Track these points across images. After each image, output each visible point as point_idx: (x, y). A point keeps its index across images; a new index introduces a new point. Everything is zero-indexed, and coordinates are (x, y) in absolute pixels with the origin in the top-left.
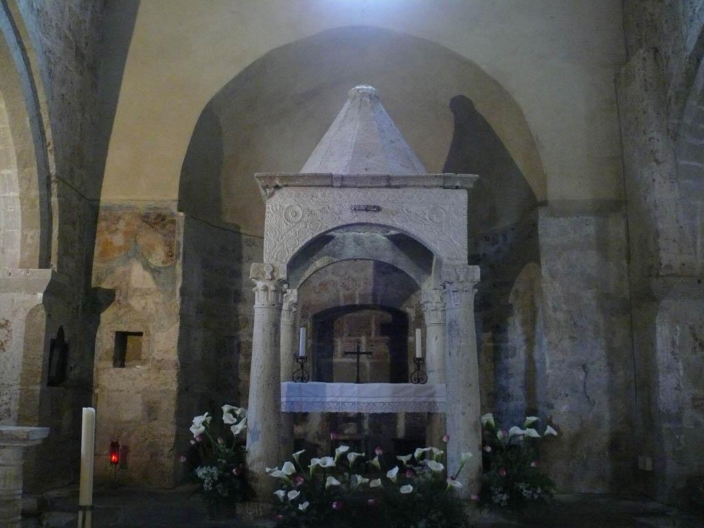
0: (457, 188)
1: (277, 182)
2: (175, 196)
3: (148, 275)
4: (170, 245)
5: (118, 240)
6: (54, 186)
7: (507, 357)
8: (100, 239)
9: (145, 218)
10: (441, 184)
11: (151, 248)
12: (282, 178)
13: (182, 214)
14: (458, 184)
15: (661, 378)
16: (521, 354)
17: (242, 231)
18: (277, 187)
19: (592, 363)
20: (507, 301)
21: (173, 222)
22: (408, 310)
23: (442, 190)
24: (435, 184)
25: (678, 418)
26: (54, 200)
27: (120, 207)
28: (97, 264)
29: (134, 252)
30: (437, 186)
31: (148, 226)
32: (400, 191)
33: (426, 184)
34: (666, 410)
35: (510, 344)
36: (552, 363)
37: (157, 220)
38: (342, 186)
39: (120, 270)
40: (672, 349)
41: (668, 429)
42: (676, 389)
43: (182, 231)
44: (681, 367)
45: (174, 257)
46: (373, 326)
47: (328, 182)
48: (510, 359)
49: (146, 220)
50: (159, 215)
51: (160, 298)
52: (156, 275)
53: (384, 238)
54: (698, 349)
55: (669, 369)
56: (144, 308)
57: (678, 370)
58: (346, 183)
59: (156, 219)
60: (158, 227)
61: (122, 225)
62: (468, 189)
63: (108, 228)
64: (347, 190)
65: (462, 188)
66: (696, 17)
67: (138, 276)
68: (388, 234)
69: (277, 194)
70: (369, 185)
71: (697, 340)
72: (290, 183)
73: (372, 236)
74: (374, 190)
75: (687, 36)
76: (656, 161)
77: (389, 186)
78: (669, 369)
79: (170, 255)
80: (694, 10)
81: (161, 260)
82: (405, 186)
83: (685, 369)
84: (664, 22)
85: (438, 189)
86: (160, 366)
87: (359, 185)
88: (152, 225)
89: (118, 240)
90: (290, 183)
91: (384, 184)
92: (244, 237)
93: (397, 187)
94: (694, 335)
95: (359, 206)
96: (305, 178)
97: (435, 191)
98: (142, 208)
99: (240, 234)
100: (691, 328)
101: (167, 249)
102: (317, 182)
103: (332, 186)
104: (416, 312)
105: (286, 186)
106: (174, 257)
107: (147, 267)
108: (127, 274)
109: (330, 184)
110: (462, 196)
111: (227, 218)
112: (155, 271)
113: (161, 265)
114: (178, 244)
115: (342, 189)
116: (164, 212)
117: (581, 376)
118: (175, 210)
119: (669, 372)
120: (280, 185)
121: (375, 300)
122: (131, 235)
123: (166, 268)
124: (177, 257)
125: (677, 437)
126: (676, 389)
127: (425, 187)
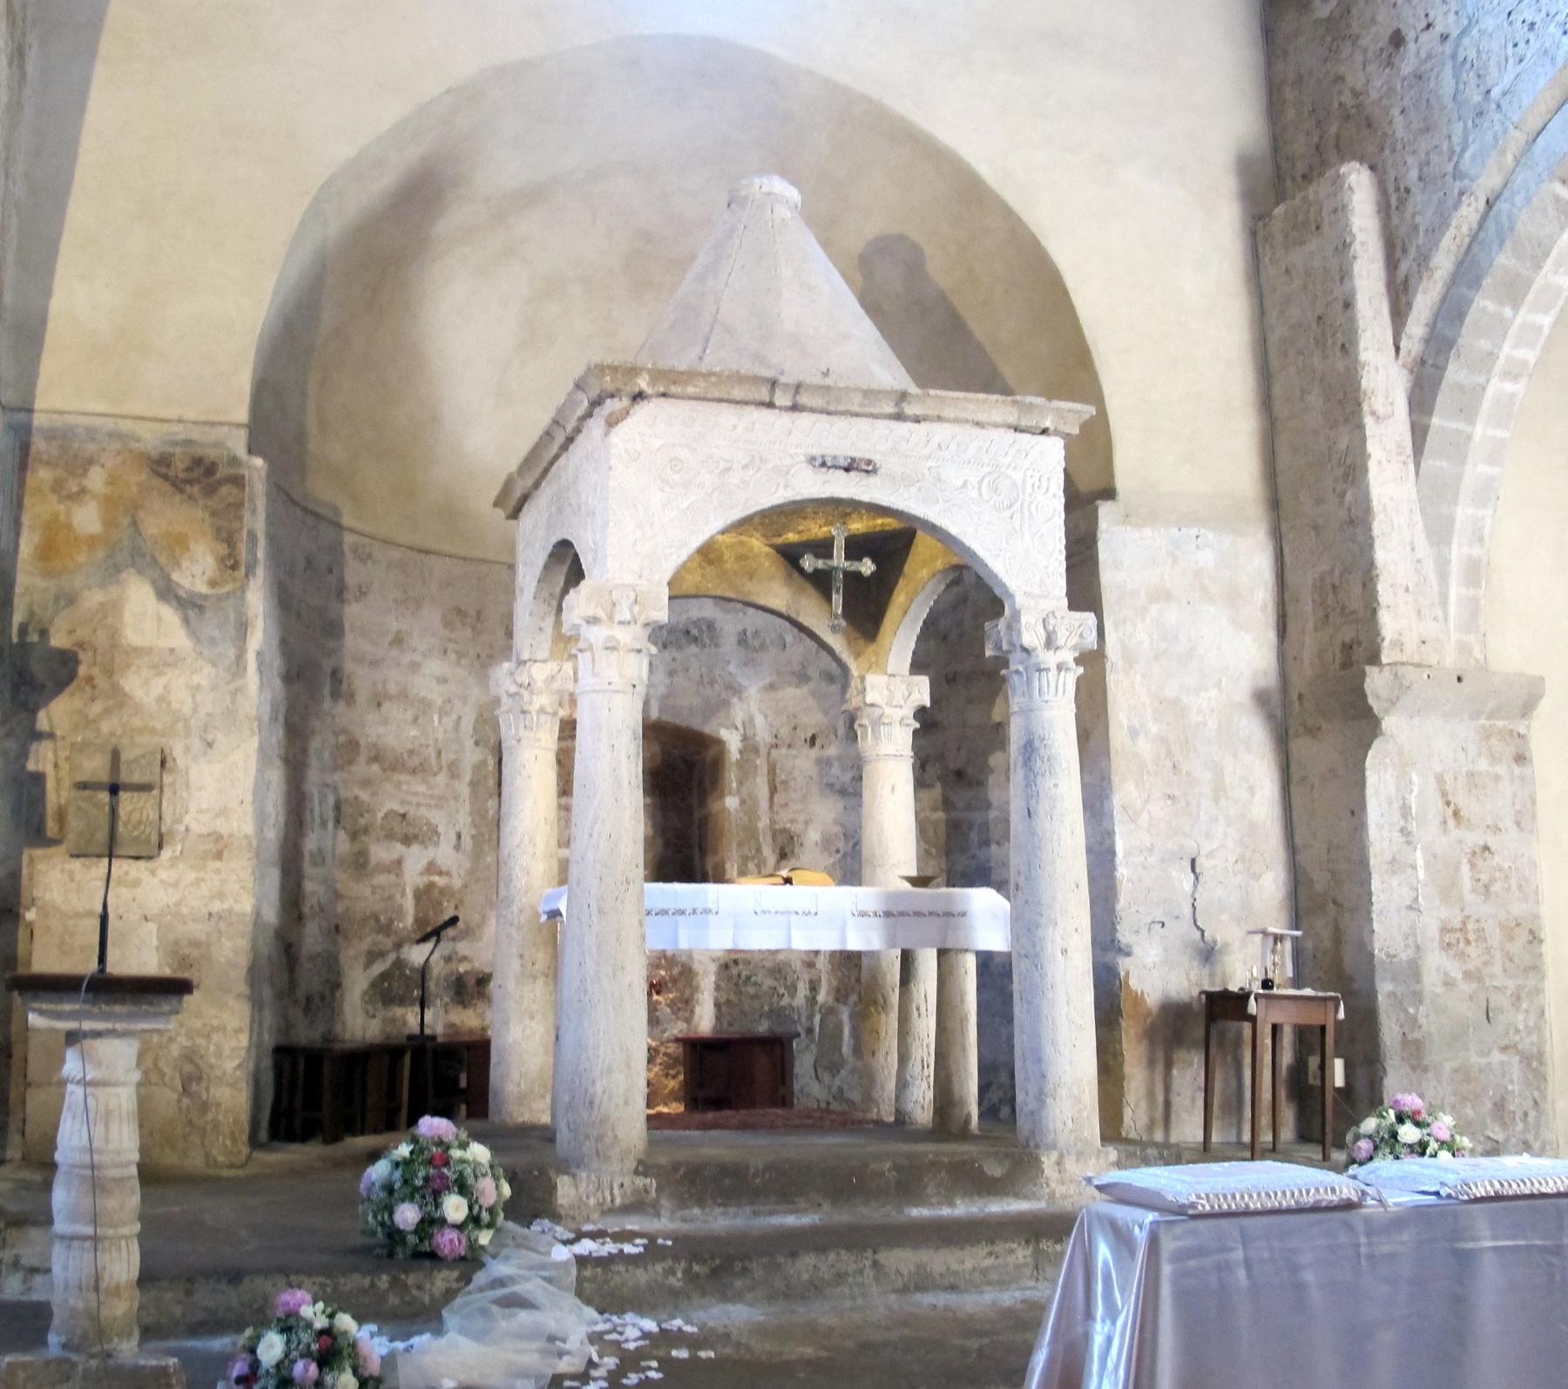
0: (1044, 432)
1: (643, 383)
2: (242, 414)
3: (170, 615)
4: (230, 540)
5: (87, 519)
7: (986, 843)
8: (36, 511)
9: (159, 465)
10: (1012, 420)
11: (178, 544)
12: (658, 375)
13: (259, 462)
14: (1048, 424)
15: (1375, 885)
17: (347, 520)
18: (639, 396)
19: (1210, 855)
20: (989, 716)
22: (724, 734)
23: (1011, 434)
24: (999, 419)
25: (1414, 970)
27: (92, 433)
29: (129, 551)
30: (996, 426)
31: (166, 486)
32: (923, 428)
33: (981, 417)
34: (1388, 955)
35: (992, 814)
36: (1128, 854)
37: (194, 474)
38: (795, 408)
39: (93, 598)
40: (1402, 823)
41: (1392, 994)
42: (1410, 908)
43: (261, 504)
44: (1420, 863)
45: (243, 570)
47: (764, 394)
48: (994, 847)
49: (163, 470)
50: (198, 461)
51: (204, 675)
52: (191, 613)
53: (767, 549)
54: (1451, 823)
55: (1395, 865)
56: (161, 699)
57: (1414, 867)
58: (804, 399)
59: (189, 469)
60: (195, 490)
62: (1067, 437)
63: (58, 486)
64: (805, 419)
65: (1057, 433)
66: (1493, 106)
67: (142, 615)
68: (779, 541)
69: (643, 411)
70: (855, 409)
71: (1448, 804)
72: (674, 389)
73: (741, 543)
74: (864, 423)
75: (1463, 151)
76: (1373, 413)
77: (899, 417)
78: (1395, 865)
79: (229, 563)
80: (1488, 92)
81: (205, 578)
82: (939, 419)
83: (1428, 864)
84: (1396, 112)
85: (1002, 431)
86: (218, 848)
87: (832, 408)
88: (178, 485)
90: (674, 389)
91: (889, 408)
92: (349, 539)
93: (917, 420)
94: (1444, 794)
95: (835, 458)
96: (714, 379)
97: (996, 434)
98: (150, 438)
99: (338, 526)
100: (1440, 779)
101: (223, 549)
102: (737, 393)
103: (770, 405)
104: (745, 738)
105: (664, 395)
106: (243, 570)
107: (166, 591)
108: (111, 609)
109: (767, 399)
112: (189, 606)
113: (203, 589)
114: (252, 537)
115: (796, 415)
116: (212, 454)
118: (241, 451)
119: (1394, 873)
120: (649, 391)
123: (220, 598)
124: (250, 571)
125: (1411, 1011)
126: (1410, 908)
127: (978, 424)
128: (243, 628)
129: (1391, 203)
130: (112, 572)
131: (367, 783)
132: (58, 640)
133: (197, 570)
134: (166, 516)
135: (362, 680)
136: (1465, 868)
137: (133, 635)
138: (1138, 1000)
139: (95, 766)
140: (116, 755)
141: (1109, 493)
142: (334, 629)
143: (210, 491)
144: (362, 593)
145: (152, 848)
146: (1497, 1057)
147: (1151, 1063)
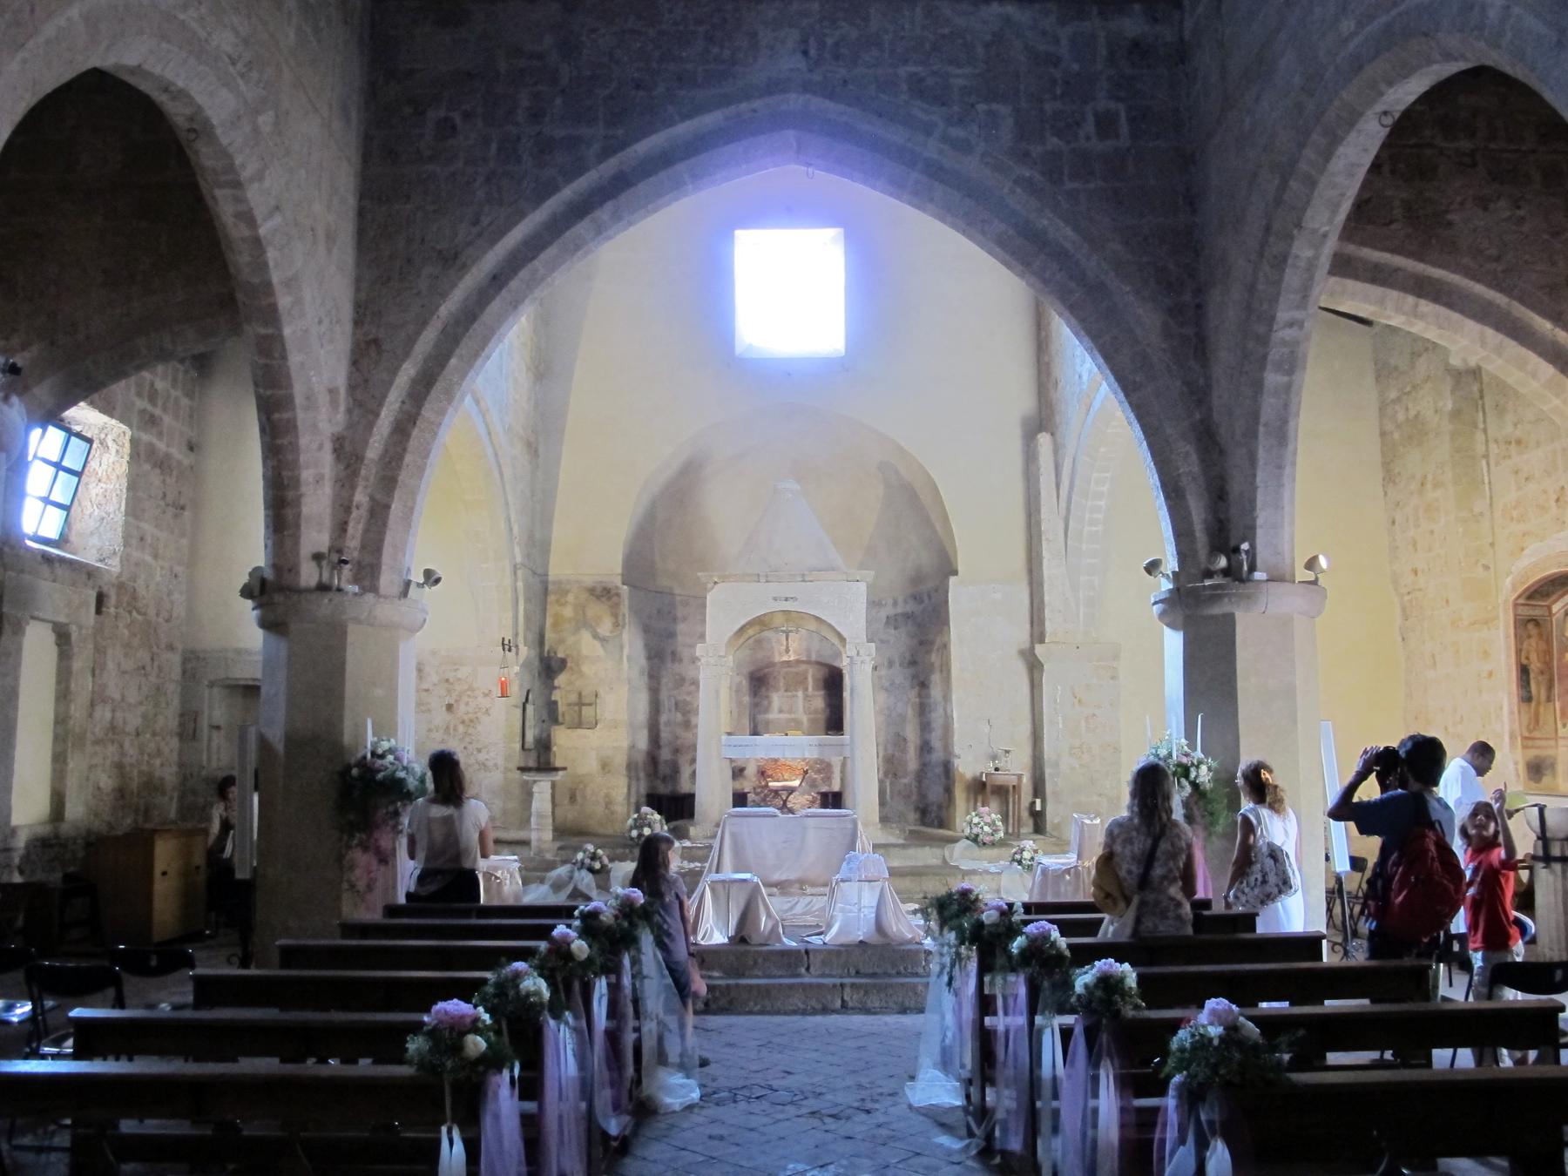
2: (619, 570)
3: (597, 644)
4: (615, 615)
6: (520, 573)
9: (592, 591)
16: (940, 711)
21: (618, 595)
25: (1057, 765)
26: (520, 584)
28: (549, 636)
29: (582, 622)
37: (604, 593)
39: (571, 640)
46: (810, 680)
61: (570, 598)
67: (587, 644)
79: (616, 625)
88: (598, 598)
89: (568, 612)
98: (588, 582)
107: (596, 636)
110: (863, 587)
111: (664, 582)
112: (603, 640)
117: (987, 729)
118: (619, 582)
121: (809, 655)
122: (580, 608)
128: (622, 647)
129: (1057, 449)
130: (577, 630)
131: (689, 693)
132: (560, 655)
133: (605, 628)
134: (596, 609)
135: (685, 653)
136: (1083, 724)
137: (585, 652)
138: (962, 775)
139: (573, 698)
140: (580, 695)
141: (955, 573)
142: (671, 635)
143: (609, 599)
144: (685, 619)
145: (593, 725)
146: (1095, 798)
147: (968, 800)
